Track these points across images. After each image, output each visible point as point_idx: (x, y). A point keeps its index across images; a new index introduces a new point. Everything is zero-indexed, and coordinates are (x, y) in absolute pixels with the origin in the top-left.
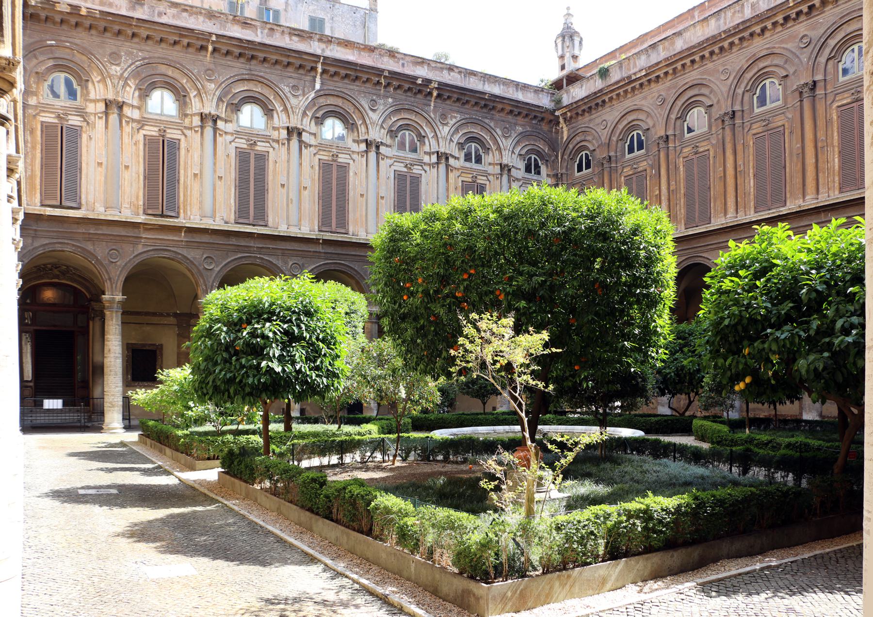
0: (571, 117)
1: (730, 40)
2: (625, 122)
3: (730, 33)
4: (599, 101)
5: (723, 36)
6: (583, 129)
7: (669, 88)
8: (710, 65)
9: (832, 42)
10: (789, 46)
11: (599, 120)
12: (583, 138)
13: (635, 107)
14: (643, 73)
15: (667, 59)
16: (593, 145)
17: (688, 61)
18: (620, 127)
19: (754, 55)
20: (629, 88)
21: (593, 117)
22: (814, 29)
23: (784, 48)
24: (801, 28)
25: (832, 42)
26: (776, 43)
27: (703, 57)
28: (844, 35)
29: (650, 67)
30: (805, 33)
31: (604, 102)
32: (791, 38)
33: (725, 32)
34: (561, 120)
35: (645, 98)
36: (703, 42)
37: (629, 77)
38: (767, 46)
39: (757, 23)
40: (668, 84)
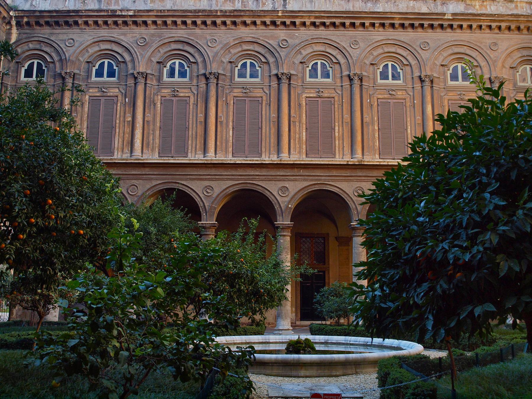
0: (28, 23)
1: (223, 19)
2: (97, 48)
3: (225, 14)
4: (71, 20)
5: (219, 14)
6: (41, 39)
7: (153, 35)
8: (198, 31)
9: (304, 53)
10: (270, 42)
11: (61, 37)
12: (38, 47)
13: (112, 39)
14: (131, 13)
15: (158, 11)
16: (51, 57)
17: (179, 21)
18: (91, 51)
19: (241, 38)
20: (110, 21)
21: (55, 31)
22: (291, 38)
23: (267, 42)
24: (281, 33)
25: (304, 53)
26: (261, 36)
27: (194, 23)
28: (312, 50)
29: (139, 11)
30: (285, 38)
31: (76, 23)
32: (273, 37)
33: (221, 11)
34: (14, 23)
35: (124, 34)
36: (199, 11)
37: (115, 11)
38: (253, 36)
39: (249, 16)
40: (152, 31)
